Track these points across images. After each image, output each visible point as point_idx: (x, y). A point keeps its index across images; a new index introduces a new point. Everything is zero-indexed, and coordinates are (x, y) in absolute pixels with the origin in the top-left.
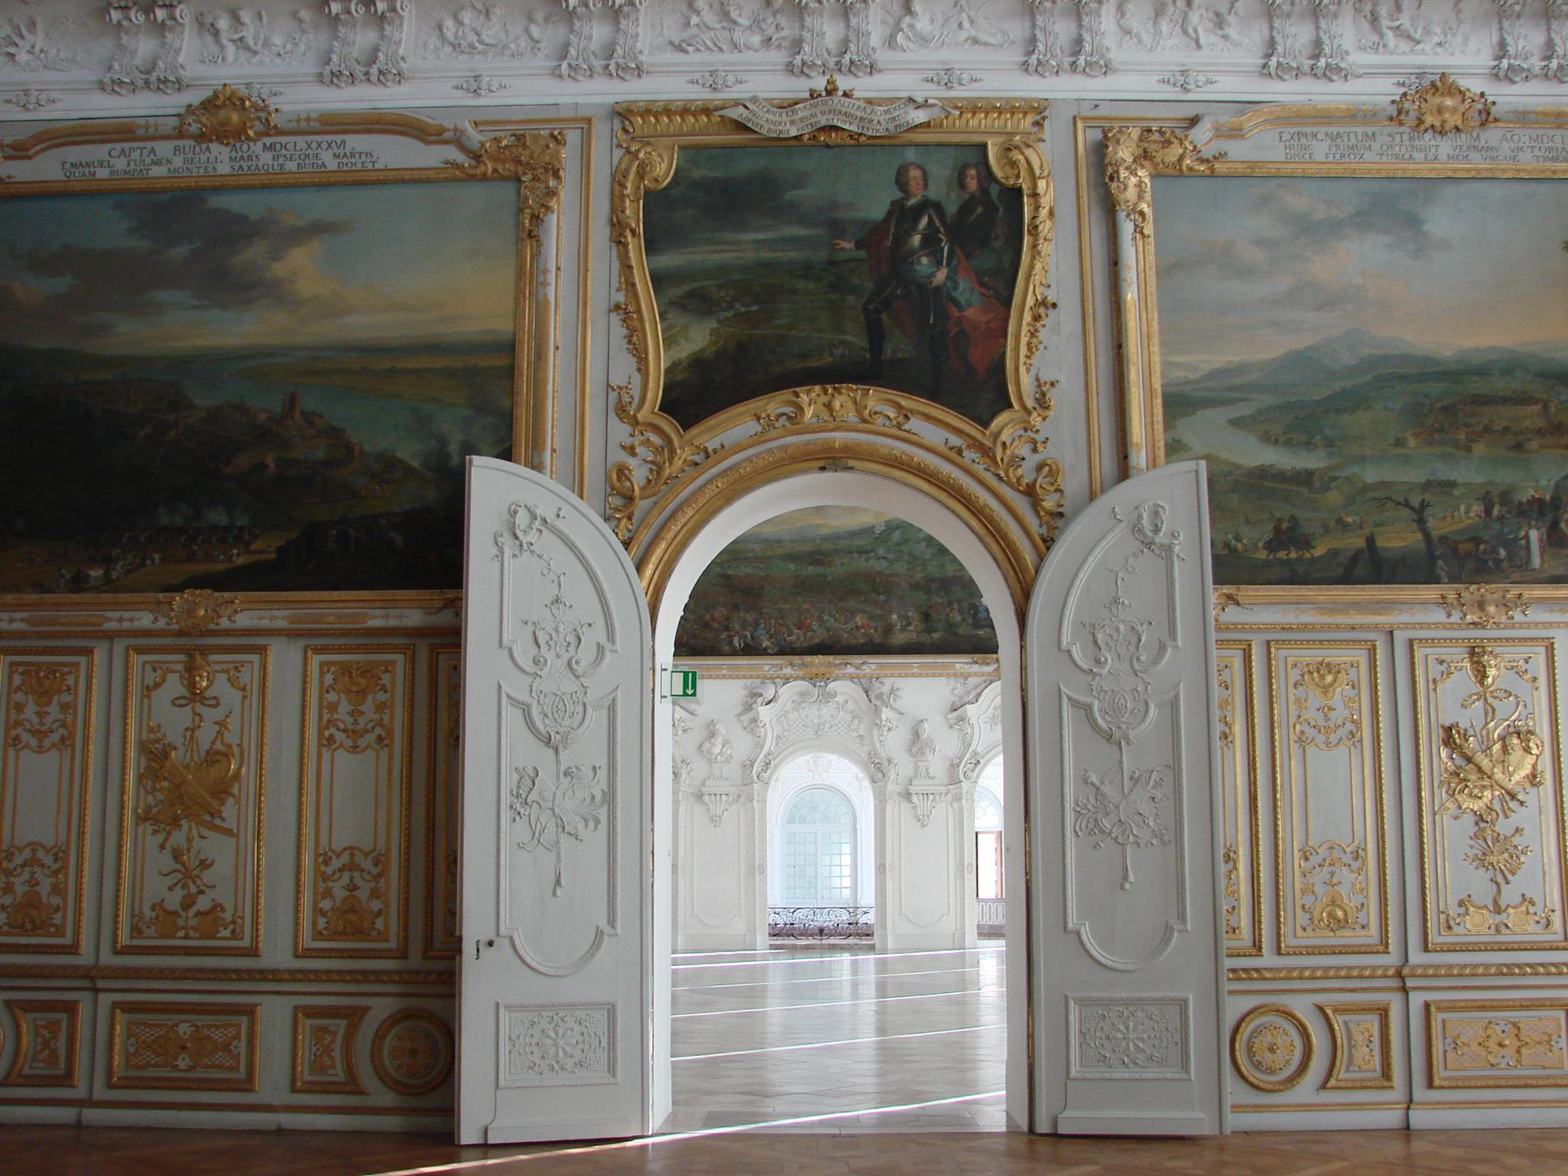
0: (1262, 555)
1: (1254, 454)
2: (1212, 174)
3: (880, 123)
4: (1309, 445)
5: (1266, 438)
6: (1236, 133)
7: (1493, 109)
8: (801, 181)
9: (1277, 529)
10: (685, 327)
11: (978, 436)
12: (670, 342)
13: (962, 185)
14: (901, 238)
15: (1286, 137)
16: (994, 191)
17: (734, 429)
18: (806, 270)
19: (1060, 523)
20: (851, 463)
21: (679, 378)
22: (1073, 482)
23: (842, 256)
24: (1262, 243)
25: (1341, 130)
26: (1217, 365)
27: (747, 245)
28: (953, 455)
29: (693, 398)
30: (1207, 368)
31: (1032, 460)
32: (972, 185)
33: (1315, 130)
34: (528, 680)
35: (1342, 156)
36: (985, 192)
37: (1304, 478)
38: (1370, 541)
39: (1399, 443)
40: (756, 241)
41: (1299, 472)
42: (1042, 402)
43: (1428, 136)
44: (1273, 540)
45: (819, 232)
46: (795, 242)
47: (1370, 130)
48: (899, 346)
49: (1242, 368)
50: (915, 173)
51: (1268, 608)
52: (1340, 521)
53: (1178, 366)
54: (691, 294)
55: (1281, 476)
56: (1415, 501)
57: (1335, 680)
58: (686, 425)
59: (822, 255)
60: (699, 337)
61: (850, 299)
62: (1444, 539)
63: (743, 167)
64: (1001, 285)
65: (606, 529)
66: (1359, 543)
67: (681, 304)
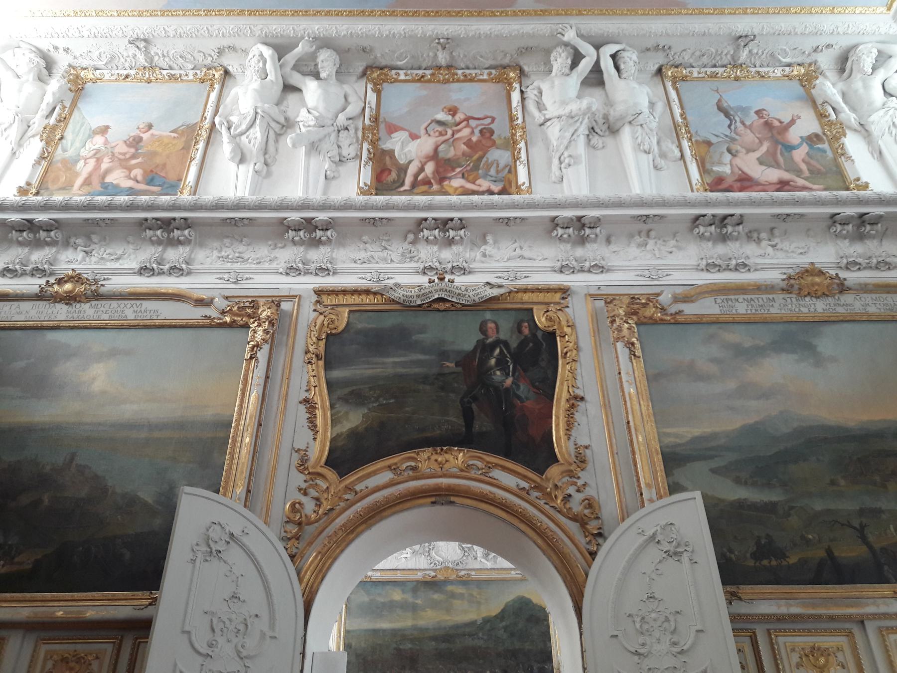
0: (751, 563)
1: (732, 492)
2: (677, 323)
3: (472, 296)
4: (768, 485)
5: (738, 481)
6: (687, 299)
7: (846, 283)
8: (422, 330)
9: (758, 544)
10: (347, 413)
11: (538, 480)
12: (334, 422)
13: (520, 331)
14: (483, 361)
15: (719, 301)
16: (539, 334)
17: (377, 479)
18: (425, 379)
19: (600, 541)
20: (452, 499)
21: (340, 444)
22: (609, 507)
23: (446, 371)
24: (713, 360)
25: (753, 297)
26: (696, 434)
27: (390, 364)
28: (524, 494)
29: (346, 457)
30: (690, 436)
31: (578, 497)
32: (526, 331)
33: (737, 297)
34: (200, 660)
35: (756, 310)
36: (534, 335)
37: (771, 508)
38: (829, 552)
39: (833, 483)
40: (395, 363)
41: (766, 503)
42: (582, 461)
43: (807, 299)
44: (750, 554)
45: (433, 357)
46: (418, 363)
47: (771, 296)
48: (483, 423)
49: (714, 436)
50: (491, 325)
51: (767, 603)
52: (803, 537)
53: (668, 435)
54: (352, 393)
55: (754, 507)
56: (856, 523)
57: (827, 661)
58: (342, 474)
59: (435, 370)
60: (354, 419)
61: (452, 395)
62: (884, 550)
63: (389, 321)
64: (546, 388)
65: (280, 546)
66: (822, 554)
67: (345, 400)
